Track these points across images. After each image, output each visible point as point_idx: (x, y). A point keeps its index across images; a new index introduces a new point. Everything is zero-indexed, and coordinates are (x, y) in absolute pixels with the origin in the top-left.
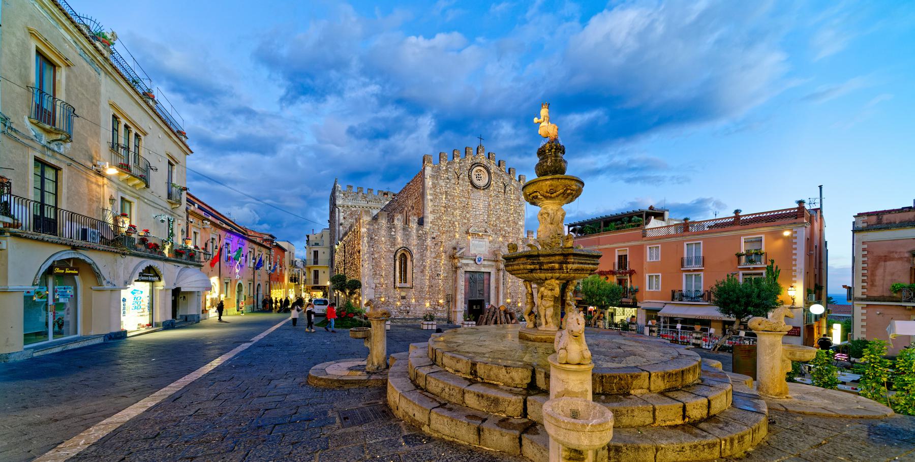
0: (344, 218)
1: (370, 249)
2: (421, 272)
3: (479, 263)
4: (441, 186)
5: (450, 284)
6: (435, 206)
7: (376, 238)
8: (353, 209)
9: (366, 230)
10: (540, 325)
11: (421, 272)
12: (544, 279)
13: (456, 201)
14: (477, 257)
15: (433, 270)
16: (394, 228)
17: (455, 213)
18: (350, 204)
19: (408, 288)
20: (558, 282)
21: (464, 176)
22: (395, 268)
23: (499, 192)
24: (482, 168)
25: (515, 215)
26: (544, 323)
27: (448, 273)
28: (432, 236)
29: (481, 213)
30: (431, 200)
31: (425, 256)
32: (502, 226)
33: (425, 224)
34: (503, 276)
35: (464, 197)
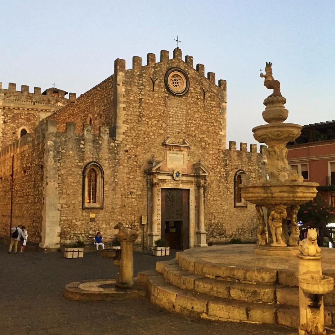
1: (56, 165)
2: (113, 190)
3: (177, 179)
4: (135, 93)
5: (145, 203)
6: (128, 115)
7: (64, 151)
8: (15, 112)
9: (52, 143)
10: (272, 242)
11: (113, 190)
12: (274, 204)
13: (151, 109)
14: (175, 172)
15: (126, 187)
16: (83, 140)
17: (150, 122)
18: (12, 105)
20: (285, 207)
21: (159, 82)
23: (198, 99)
24: (179, 73)
25: (215, 124)
26: (275, 240)
27: (142, 191)
28: (125, 148)
29: (178, 122)
31: (118, 172)
32: (201, 136)
33: (117, 136)
35: (160, 105)
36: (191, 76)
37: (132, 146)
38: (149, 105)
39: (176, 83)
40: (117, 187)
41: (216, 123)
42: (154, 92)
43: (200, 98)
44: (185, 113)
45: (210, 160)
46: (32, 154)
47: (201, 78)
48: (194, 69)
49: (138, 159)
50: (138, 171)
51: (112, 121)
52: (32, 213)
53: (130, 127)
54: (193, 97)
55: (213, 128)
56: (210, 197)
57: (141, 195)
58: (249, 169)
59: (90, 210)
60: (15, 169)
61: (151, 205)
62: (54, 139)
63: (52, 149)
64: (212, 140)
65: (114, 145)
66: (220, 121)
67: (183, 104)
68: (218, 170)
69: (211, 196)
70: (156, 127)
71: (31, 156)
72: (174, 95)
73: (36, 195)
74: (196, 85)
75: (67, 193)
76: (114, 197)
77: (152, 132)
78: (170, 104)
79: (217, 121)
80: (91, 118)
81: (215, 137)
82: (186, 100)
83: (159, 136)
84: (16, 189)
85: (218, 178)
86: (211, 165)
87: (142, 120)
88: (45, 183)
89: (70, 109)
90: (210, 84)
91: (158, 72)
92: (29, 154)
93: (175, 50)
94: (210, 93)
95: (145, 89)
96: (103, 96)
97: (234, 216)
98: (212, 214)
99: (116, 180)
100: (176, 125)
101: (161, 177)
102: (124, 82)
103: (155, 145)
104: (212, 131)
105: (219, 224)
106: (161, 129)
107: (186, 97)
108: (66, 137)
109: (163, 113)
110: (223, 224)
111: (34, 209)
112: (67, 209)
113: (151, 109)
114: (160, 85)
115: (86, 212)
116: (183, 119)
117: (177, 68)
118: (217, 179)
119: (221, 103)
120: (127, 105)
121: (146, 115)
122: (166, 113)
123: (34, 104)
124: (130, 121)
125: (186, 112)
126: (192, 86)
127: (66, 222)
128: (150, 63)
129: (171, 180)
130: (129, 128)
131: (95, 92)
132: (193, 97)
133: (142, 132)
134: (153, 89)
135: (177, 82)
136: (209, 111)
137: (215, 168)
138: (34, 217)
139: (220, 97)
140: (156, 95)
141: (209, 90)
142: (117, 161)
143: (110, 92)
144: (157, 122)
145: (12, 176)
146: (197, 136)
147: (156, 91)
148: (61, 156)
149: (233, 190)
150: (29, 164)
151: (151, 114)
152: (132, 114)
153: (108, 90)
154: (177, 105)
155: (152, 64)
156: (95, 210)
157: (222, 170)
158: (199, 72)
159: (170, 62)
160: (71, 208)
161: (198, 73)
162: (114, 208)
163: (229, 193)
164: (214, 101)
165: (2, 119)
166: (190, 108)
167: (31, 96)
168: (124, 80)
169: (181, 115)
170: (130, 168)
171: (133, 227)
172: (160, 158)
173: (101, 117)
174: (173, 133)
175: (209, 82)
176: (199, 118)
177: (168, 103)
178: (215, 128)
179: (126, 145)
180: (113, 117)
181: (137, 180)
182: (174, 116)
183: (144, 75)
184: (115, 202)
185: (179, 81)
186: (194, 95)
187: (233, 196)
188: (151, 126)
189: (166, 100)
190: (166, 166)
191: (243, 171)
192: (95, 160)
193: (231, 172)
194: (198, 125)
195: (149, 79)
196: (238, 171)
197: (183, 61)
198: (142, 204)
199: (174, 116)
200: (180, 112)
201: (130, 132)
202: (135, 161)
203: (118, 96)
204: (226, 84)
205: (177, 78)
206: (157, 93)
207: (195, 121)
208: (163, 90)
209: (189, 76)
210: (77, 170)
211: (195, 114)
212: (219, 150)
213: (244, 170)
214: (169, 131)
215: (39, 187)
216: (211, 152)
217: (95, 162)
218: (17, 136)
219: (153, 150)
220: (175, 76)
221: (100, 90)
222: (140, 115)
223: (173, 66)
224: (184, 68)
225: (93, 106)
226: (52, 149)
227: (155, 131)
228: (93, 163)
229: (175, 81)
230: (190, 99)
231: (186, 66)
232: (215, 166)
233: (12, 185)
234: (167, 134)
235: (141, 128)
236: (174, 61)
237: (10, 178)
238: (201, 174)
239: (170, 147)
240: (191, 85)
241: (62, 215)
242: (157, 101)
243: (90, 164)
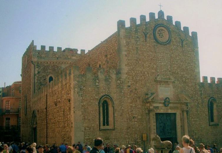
0: (39, 72)
4: (133, 44)
6: (129, 60)
13: (145, 55)
15: (130, 113)
16: (98, 79)
19: (111, 130)
21: (150, 35)
22: (99, 113)
23: (178, 46)
24: (163, 28)
25: (192, 64)
29: (165, 64)
30: (126, 56)
32: (182, 73)
34: (187, 116)
35: (151, 52)
36: (172, 29)
37: (133, 82)
39: (161, 35)
40: (123, 113)
41: (192, 63)
42: (146, 43)
43: (179, 46)
44: (169, 57)
45: (190, 91)
46: (61, 92)
48: (174, 25)
49: (137, 92)
50: (138, 101)
51: (117, 65)
52: (63, 134)
53: (131, 68)
54: (174, 45)
55: (190, 67)
56: (192, 119)
57: (141, 119)
58: (218, 96)
59: (105, 131)
60: (48, 103)
61: (149, 126)
62: (77, 79)
63: (76, 86)
64: (190, 75)
65: (120, 82)
66: (195, 62)
68: (196, 98)
69: (192, 118)
70: (149, 68)
71: (60, 93)
72: (161, 44)
73: (65, 121)
75: (88, 119)
76: (122, 121)
77: (147, 72)
80: (100, 65)
83: (152, 75)
84: (49, 118)
85: (196, 104)
86: (190, 94)
87: (138, 63)
88: (72, 112)
89: (83, 60)
92: (58, 92)
93: (159, 12)
95: (140, 40)
96: (109, 48)
97: (210, 132)
98: (193, 131)
99: (122, 108)
100: (163, 66)
101: (155, 105)
102: (125, 36)
103: (149, 81)
105: (199, 139)
106: (153, 69)
108: (86, 77)
110: (201, 139)
111: (65, 131)
112: (89, 130)
113: (145, 55)
114: (151, 37)
115: (102, 132)
116: (168, 61)
118: (195, 105)
119: (194, 48)
120: (128, 53)
121: (141, 59)
122: (156, 57)
123: (57, 59)
125: (170, 56)
126: (173, 37)
127: (88, 140)
129: (162, 106)
130: (130, 69)
131: (103, 46)
132: (174, 45)
133: (140, 72)
134: (146, 41)
137: (194, 97)
138: (65, 137)
141: (185, 39)
142: (122, 94)
143: (114, 44)
145: (46, 108)
146: (179, 73)
148: (82, 92)
149: (207, 112)
150: (59, 99)
152: (132, 59)
154: (163, 51)
156: (108, 131)
157: (199, 98)
159: (156, 21)
160: (92, 130)
161: (176, 28)
162: (122, 129)
163: (204, 115)
165: (37, 70)
166: (172, 53)
167: (55, 53)
169: (167, 58)
170: (132, 99)
171: (136, 143)
172: (154, 91)
173: (108, 63)
177: (157, 50)
178: (192, 67)
179: (128, 82)
180: (118, 62)
181: (138, 108)
182: (162, 59)
183: (139, 30)
184: (122, 125)
187: (207, 117)
190: (158, 96)
191: (213, 98)
192: (107, 94)
193: (205, 99)
194: (179, 65)
195: (143, 33)
196: (210, 98)
197: (165, 19)
198: (143, 125)
199: (162, 59)
200: (166, 56)
201: (131, 73)
202: (136, 94)
205: (162, 32)
207: (177, 62)
208: (153, 41)
209: (170, 30)
210: (94, 101)
211: (176, 57)
212: (195, 83)
213: (215, 97)
214: (158, 70)
215: (68, 115)
216: (190, 85)
217: (107, 95)
218: (47, 81)
219: (148, 85)
220: (161, 31)
221: (106, 44)
222: (137, 59)
223: (159, 23)
226: (76, 86)
228: (106, 96)
229: (160, 34)
230: (172, 46)
231: (168, 23)
232: (194, 95)
233: (47, 115)
236: (159, 20)
237: (45, 110)
238: (184, 101)
239: (160, 82)
240: (172, 36)
241: (85, 135)
242: (149, 49)
243: (104, 97)
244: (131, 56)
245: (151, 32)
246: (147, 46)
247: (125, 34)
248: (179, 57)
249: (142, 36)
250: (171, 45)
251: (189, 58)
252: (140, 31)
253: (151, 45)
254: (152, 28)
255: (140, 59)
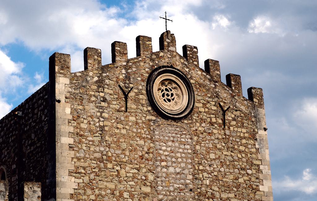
4: (91, 117)
6: (79, 159)
13: (124, 146)
17: (123, 172)
21: (137, 94)
23: (212, 124)
24: (173, 77)
25: (249, 172)
29: (178, 170)
35: (141, 138)
38: (119, 138)
39: (168, 95)
41: (250, 169)
42: (127, 114)
43: (215, 123)
44: (190, 151)
47: (215, 85)
48: (201, 69)
54: (202, 121)
55: (246, 178)
66: (258, 165)
67: (185, 134)
70: (136, 180)
74: (207, 99)
77: (128, 191)
78: (159, 135)
79: (252, 164)
81: (252, 195)
82: (191, 127)
87: (106, 167)
90: (233, 97)
91: (133, 76)
93: (162, 35)
94: (235, 113)
100: (173, 176)
104: (244, 185)
106: (145, 185)
107: (190, 121)
109: (147, 153)
113: (124, 146)
114: (139, 99)
117: (168, 67)
119: (256, 130)
124: (83, 171)
128: (117, 58)
130: (82, 185)
133: (109, 191)
134: (126, 108)
135: (170, 93)
136: (236, 147)
139: (253, 119)
140: (132, 119)
141: (231, 107)
143: (41, 117)
144: (136, 171)
146: (217, 195)
147: (132, 111)
151: (123, 156)
152: (87, 156)
153: (37, 114)
154: (174, 137)
155: (121, 61)
158: (211, 73)
159: (154, 57)
161: (208, 76)
164: (243, 126)
166: (198, 142)
168: (69, 92)
169: (183, 155)
174: (170, 192)
175: (231, 92)
176: (217, 161)
177: (157, 133)
178: (250, 179)
180: (49, 164)
182: (169, 158)
183: (107, 81)
185: (174, 91)
186: (204, 116)
188: (126, 178)
189: (152, 128)
194: (216, 173)
195: (118, 88)
197: (179, 54)
199: (169, 158)
200: (181, 150)
203: (58, 122)
204: (262, 96)
205: (169, 87)
206: (133, 114)
209: (192, 81)
211: (209, 152)
214: (160, 188)
224: (183, 68)
225: (8, 149)
227: (133, 190)
230: (198, 124)
231: (187, 63)
234: (158, 194)
235: (105, 183)
242: (135, 130)
244: (85, 148)
245: (140, 87)
246: (130, 124)
247: (70, 90)
248: (215, 153)
249: (116, 96)
250: (194, 121)
251: (244, 155)
252: (110, 81)
253: (140, 121)
254: (142, 75)
255: (109, 157)
